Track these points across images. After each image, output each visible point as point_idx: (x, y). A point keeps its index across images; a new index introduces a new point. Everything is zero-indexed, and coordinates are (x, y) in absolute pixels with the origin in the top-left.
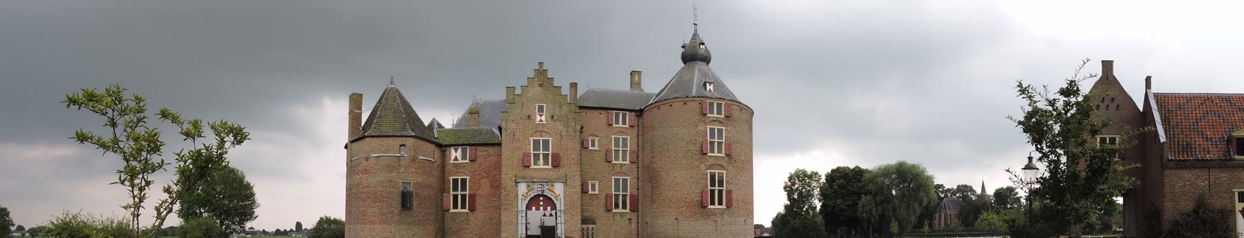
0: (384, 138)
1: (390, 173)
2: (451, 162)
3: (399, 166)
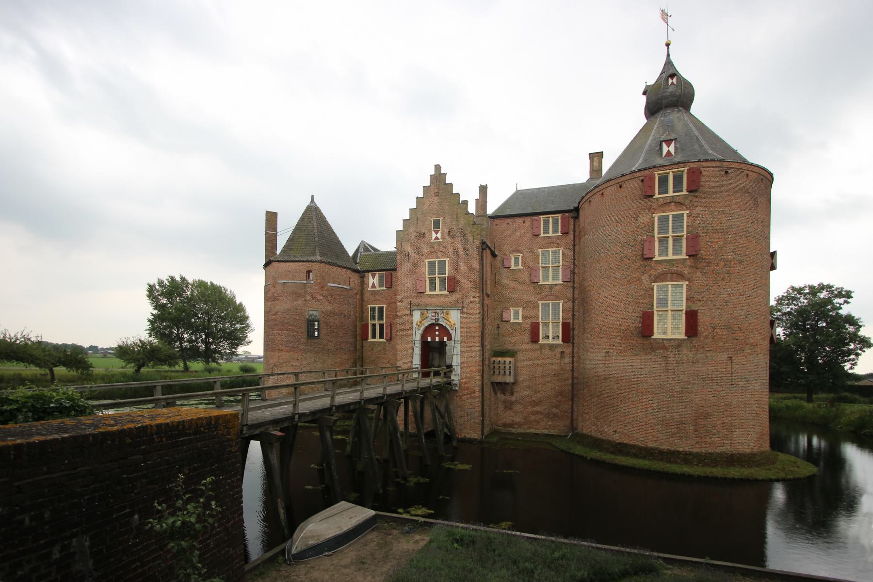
0: (291, 264)
1: (296, 300)
2: (369, 289)
3: (305, 293)
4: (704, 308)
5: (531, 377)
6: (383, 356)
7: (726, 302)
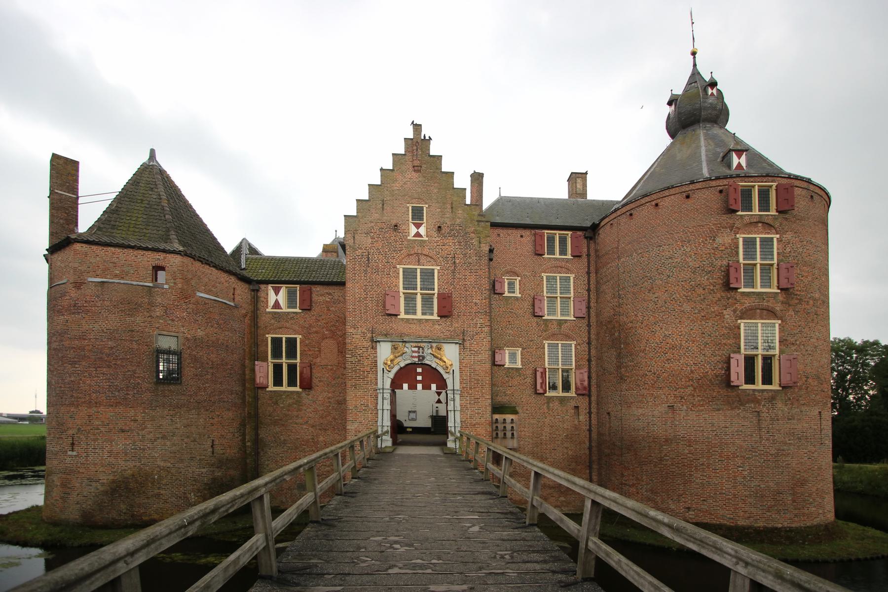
5: (536, 439)
6: (295, 413)
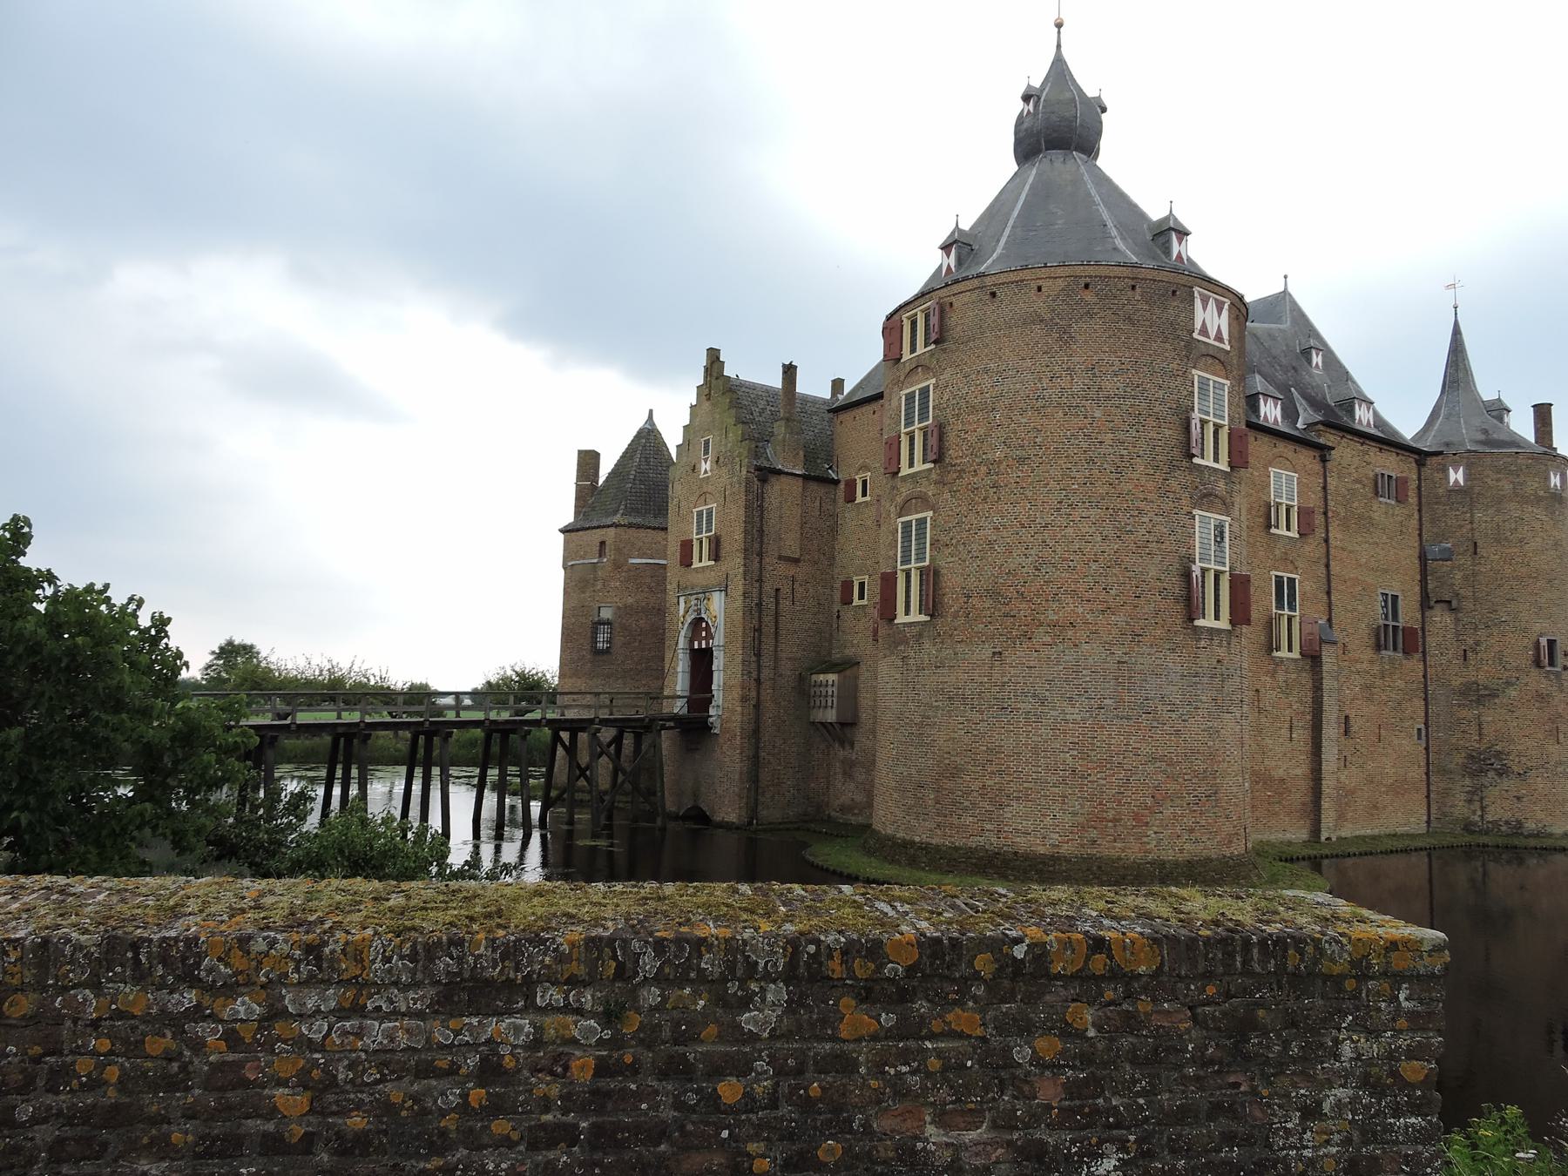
1: (583, 592)
3: (596, 579)
4: (953, 559)
7: (990, 543)
